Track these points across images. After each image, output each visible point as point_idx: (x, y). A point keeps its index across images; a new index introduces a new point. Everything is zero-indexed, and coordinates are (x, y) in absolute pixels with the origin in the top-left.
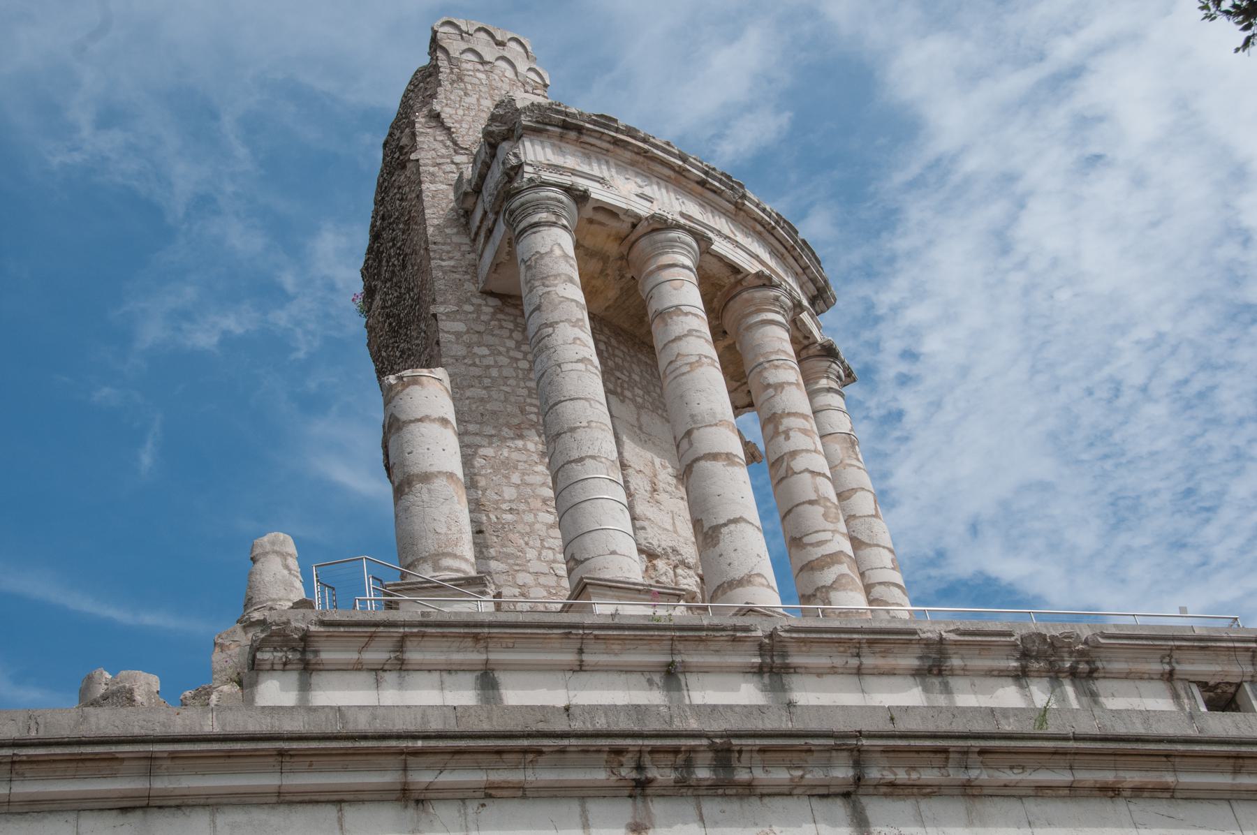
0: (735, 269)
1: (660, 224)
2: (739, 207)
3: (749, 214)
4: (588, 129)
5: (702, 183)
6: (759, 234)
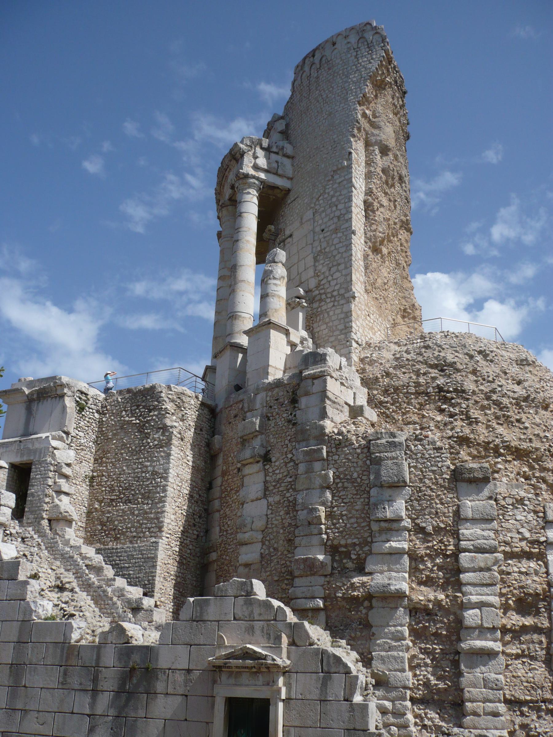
6: (224, 186)
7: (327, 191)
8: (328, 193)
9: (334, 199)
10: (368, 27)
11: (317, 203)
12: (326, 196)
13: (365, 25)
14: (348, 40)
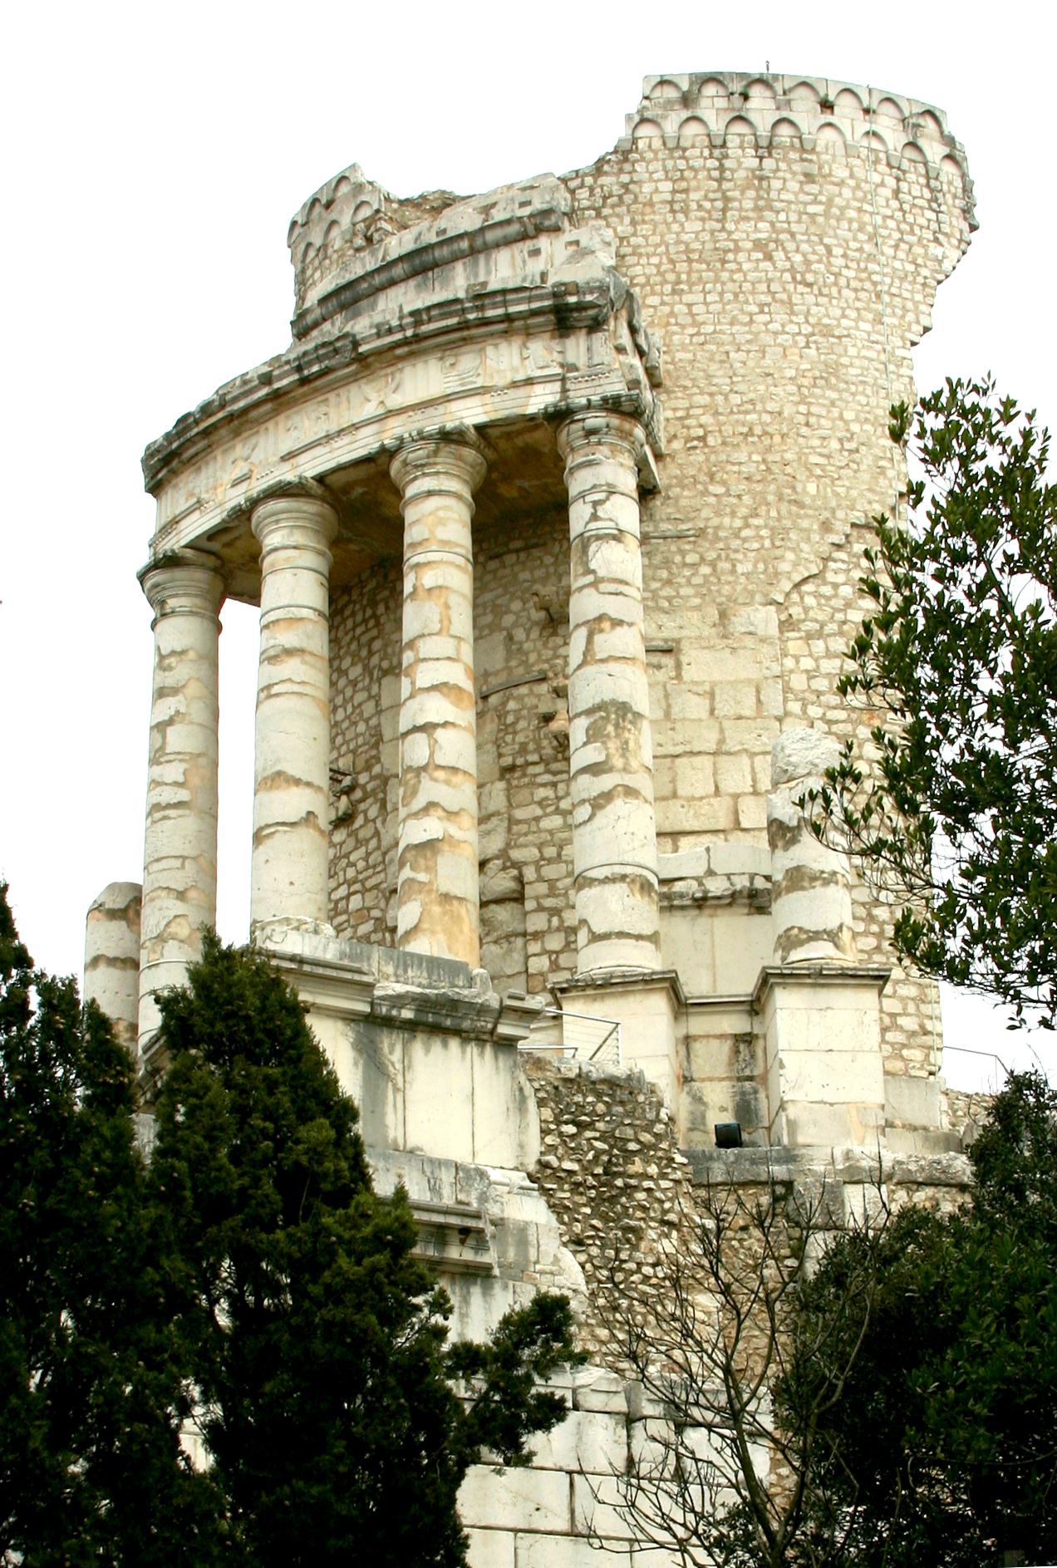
0: (368, 460)
1: (243, 514)
2: (361, 359)
3: (378, 353)
4: (179, 447)
5: (304, 381)
6: (411, 355)
10: (929, 123)
11: (795, 597)
12: (827, 590)
13: (923, 113)
14: (875, 128)
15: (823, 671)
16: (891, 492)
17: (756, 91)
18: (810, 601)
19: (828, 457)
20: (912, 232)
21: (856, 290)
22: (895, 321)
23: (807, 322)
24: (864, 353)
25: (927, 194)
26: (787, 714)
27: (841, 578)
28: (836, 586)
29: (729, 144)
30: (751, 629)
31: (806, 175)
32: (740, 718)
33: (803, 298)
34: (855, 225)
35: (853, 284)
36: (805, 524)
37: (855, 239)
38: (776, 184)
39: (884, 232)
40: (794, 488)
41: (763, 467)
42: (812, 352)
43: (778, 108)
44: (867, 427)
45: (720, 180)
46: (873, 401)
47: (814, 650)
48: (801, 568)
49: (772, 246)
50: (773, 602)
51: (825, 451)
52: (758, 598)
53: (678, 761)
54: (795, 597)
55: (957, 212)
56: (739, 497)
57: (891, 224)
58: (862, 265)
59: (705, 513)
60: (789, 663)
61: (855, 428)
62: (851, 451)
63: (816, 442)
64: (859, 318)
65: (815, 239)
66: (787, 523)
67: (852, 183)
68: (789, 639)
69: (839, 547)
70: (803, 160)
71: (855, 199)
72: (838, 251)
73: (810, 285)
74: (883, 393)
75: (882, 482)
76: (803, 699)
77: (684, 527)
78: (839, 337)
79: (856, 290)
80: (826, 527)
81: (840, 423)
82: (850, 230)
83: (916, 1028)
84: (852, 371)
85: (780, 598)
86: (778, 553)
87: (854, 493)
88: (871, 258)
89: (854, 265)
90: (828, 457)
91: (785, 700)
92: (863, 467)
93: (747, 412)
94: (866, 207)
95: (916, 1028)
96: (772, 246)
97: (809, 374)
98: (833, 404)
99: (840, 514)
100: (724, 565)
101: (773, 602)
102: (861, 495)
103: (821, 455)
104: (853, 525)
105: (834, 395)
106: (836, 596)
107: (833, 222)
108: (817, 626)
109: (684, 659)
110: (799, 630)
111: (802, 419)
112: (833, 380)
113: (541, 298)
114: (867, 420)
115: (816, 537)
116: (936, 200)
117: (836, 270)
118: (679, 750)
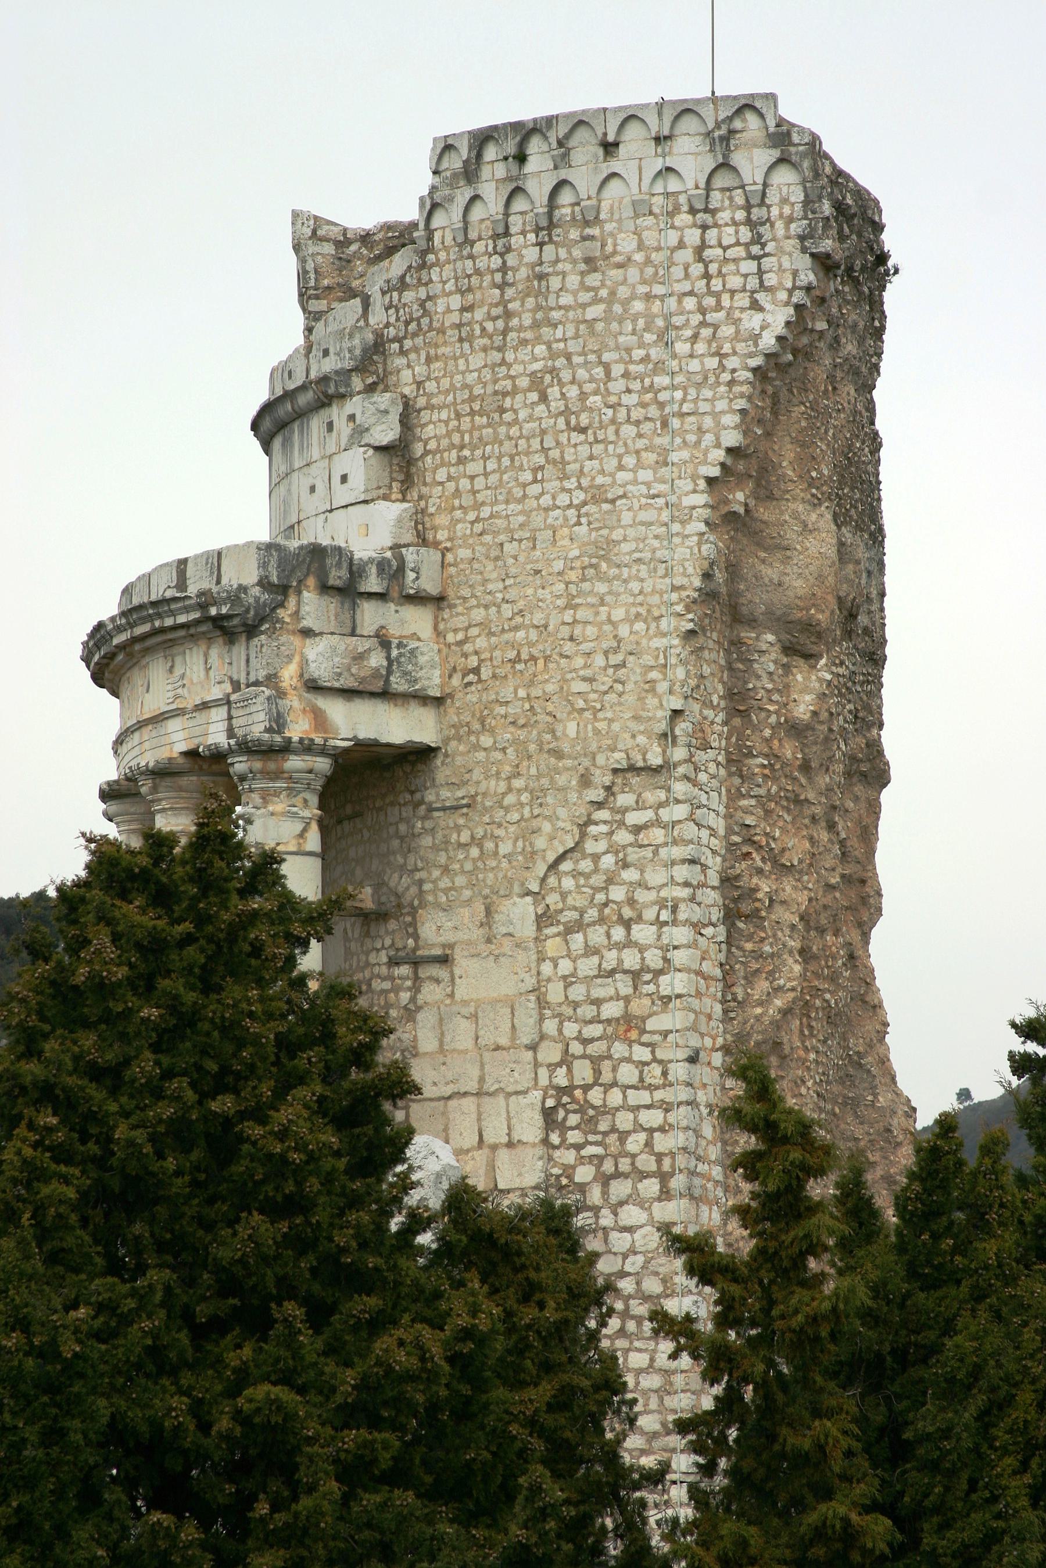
7: (590, 846)
8: (596, 858)
9: (618, 893)
12: (586, 865)
13: (739, 111)
15: (581, 974)
16: (660, 714)
17: (535, 146)
18: (568, 883)
19: (590, 680)
20: (719, 307)
21: (638, 423)
22: (685, 454)
23: (580, 487)
24: (643, 516)
25: (745, 234)
26: (543, 1037)
27: (601, 846)
28: (596, 858)
29: (513, 230)
30: (511, 930)
31: (588, 260)
32: (498, 1048)
33: (576, 450)
34: (641, 323)
35: (635, 415)
36: (561, 780)
37: (641, 345)
38: (555, 283)
39: (678, 320)
40: (553, 732)
41: (527, 706)
42: (584, 529)
43: (556, 168)
44: (640, 626)
45: (502, 286)
46: (648, 586)
47: (573, 947)
48: (556, 842)
49: (548, 378)
50: (529, 893)
51: (587, 673)
52: (517, 889)
53: (453, 1103)
54: (552, 881)
55: (791, 245)
56: (504, 750)
57: (690, 303)
58: (647, 381)
59: (477, 775)
60: (547, 968)
61: (624, 631)
62: (617, 667)
63: (579, 662)
64: (639, 465)
65: (592, 357)
66: (545, 782)
67: (639, 257)
68: (548, 937)
69: (599, 805)
70: (585, 238)
71: (644, 282)
72: (617, 370)
73: (583, 430)
74: (661, 569)
75: (651, 701)
76: (560, 1015)
77: (460, 794)
78: (613, 501)
79: (638, 423)
80: (585, 781)
81: (607, 628)
82: (634, 332)
83: (657, 1427)
84: (625, 547)
85: (535, 887)
86: (535, 823)
87: (616, 727)
88: (659, 368)
89: (636, 385)
90: (590, 680)
91: (542, 1019)
92: (630, 686)
93: (516, 628)
94: (659, 290)
95: (657, 1427)
96: (548, 378)
97: (577, 564)
98: (602, 603)
99: (601, 760)
100: (489, 845)
101: (529, 893)
102: (625, 728)
103: (584, 679)
104: (615, 771)
105: (601, 588)
106: (596, 870)
107: (614, 326)
108: (575, 915)
109: (457, 972)
110: (558, 922)
111: (565, 631)
112: (604, 566)
113: (187, 610)
114: (638, 615)
115: (573, 797)
116: (758, 239)
117: (613, 399)
118: (448, 1090)
